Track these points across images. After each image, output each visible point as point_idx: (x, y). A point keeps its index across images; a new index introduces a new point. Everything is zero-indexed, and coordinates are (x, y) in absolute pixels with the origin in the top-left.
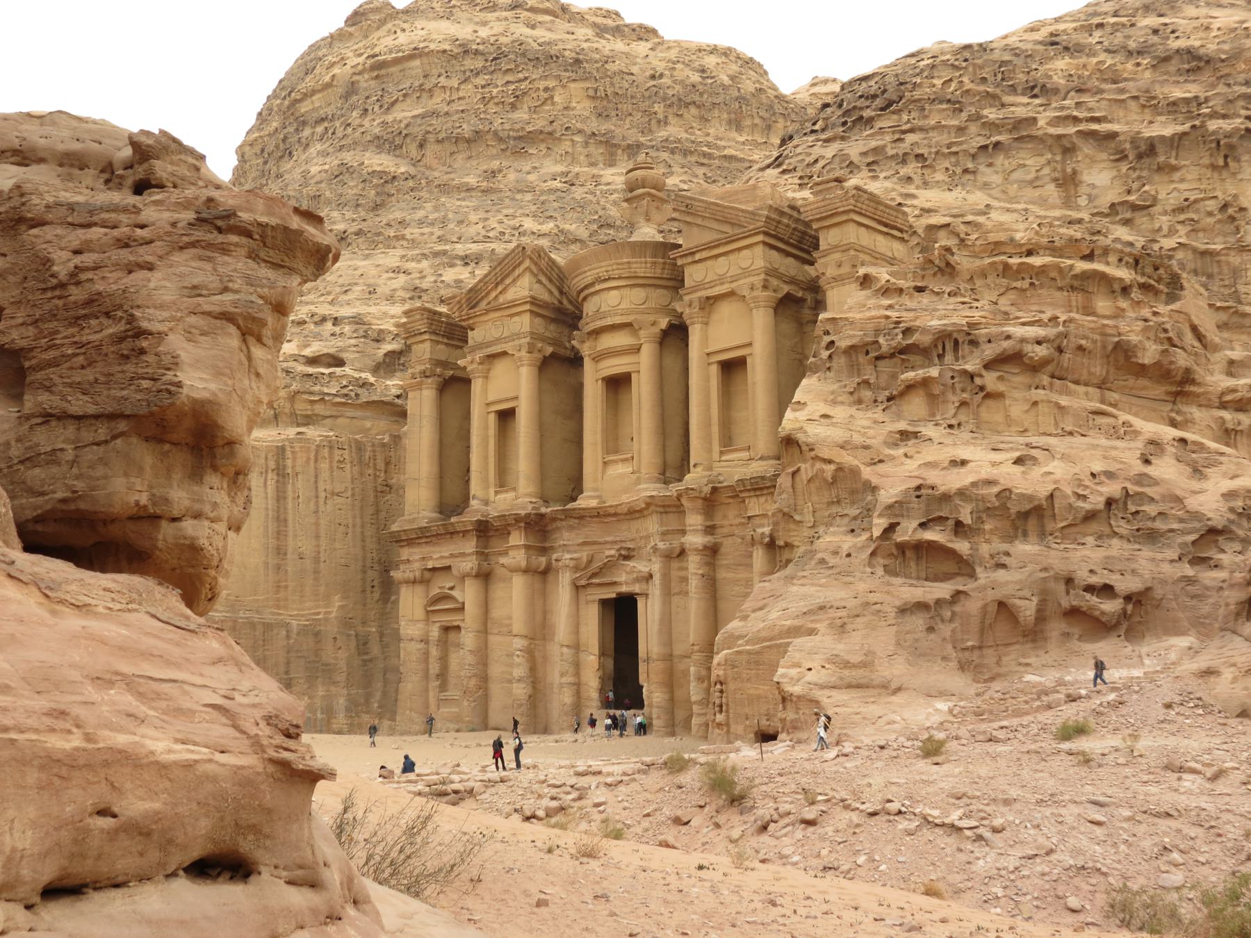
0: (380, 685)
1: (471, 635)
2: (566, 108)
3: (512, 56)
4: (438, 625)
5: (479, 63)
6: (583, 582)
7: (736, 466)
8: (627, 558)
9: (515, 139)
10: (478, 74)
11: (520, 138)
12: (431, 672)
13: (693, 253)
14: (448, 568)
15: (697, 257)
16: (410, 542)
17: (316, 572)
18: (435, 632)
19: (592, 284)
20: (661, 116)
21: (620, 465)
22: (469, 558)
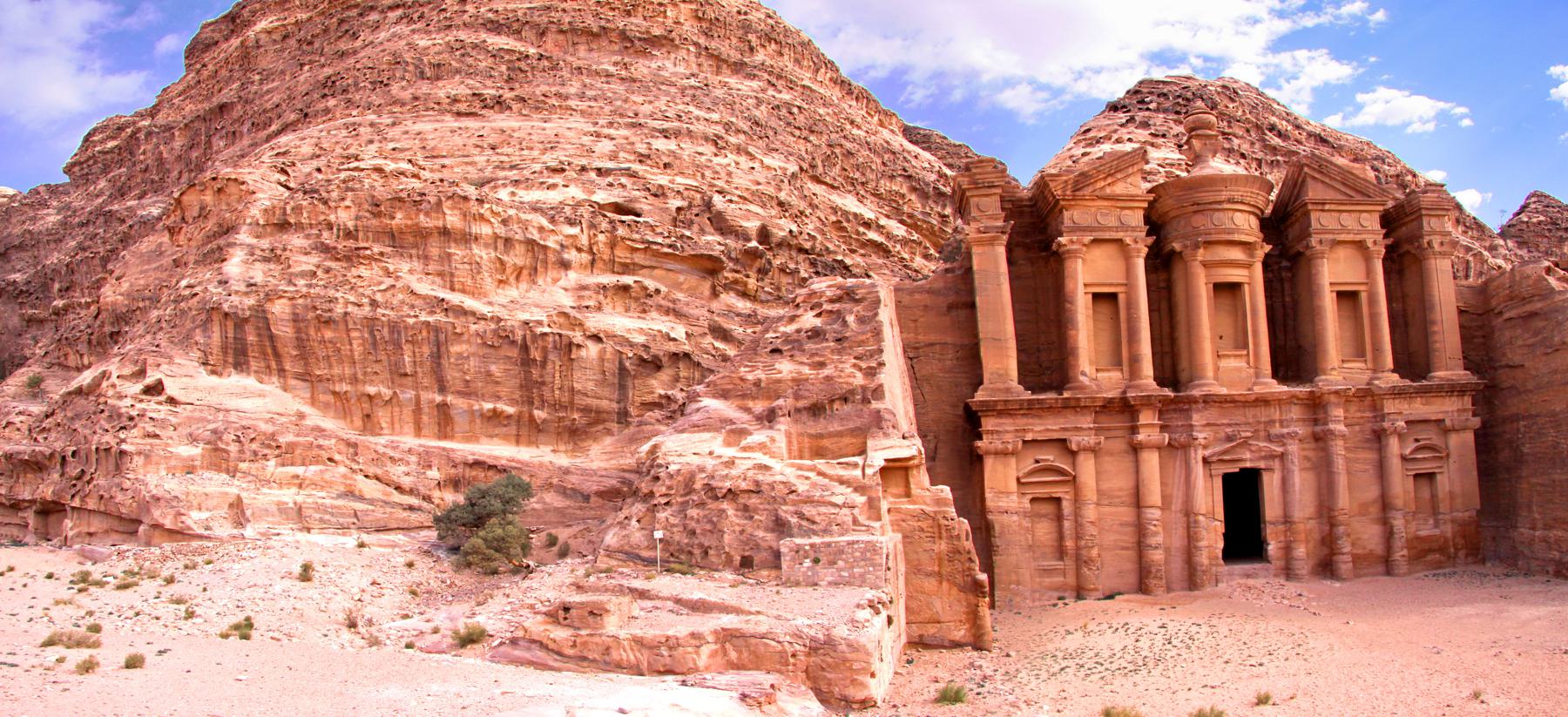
4: (1030, 497)
6: (1215, 459)
16: (1001, 413)
21: (1232, 360)
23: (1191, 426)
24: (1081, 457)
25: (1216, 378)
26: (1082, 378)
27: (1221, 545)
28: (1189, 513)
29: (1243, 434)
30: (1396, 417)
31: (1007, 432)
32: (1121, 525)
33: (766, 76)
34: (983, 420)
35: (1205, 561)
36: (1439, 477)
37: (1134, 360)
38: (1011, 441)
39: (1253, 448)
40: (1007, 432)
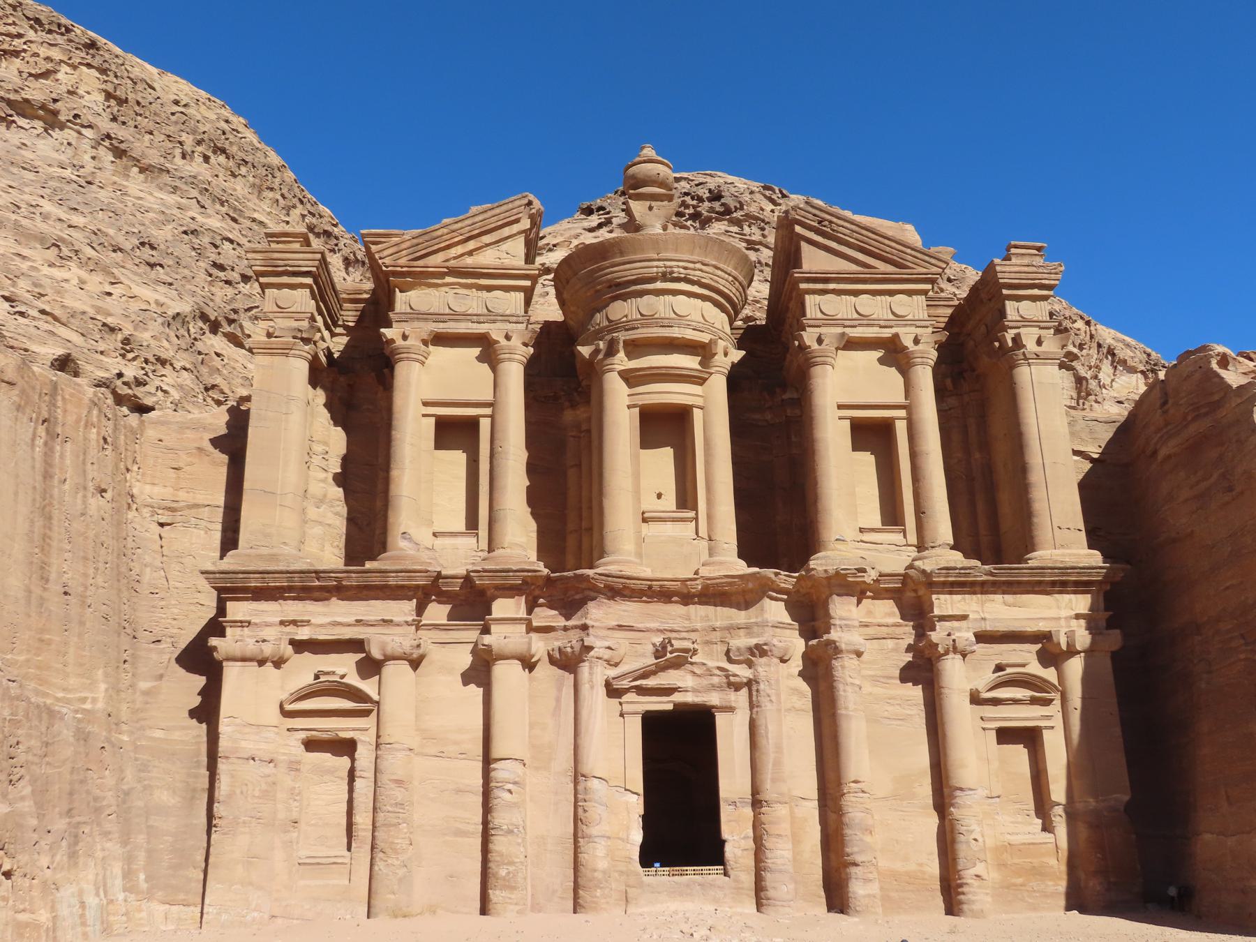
0: (141, 839)
1: (400, 755)
2: (69, 92)
4: (303, 735)
6: (625, 684)
7: (889, 551)
8: (695, 652)
12: (281, 815)
13: (826, 281)
14: (356, 645)
15: (832, 286)
16: (261, 594)
20: (188, 148)
23: (585, 628)
24: (390, 670)
25: (639, 555)
26: (403, 544)
27: (637, 836)
28: (578, 776)
29: (677, 644)
30: (955, 624)
31: (268, 625)
33: (195, 193)
34: (231, 606)
35: (602, 864)
36: (1047, 736)
38: (275, 640)
40: (268, 625)
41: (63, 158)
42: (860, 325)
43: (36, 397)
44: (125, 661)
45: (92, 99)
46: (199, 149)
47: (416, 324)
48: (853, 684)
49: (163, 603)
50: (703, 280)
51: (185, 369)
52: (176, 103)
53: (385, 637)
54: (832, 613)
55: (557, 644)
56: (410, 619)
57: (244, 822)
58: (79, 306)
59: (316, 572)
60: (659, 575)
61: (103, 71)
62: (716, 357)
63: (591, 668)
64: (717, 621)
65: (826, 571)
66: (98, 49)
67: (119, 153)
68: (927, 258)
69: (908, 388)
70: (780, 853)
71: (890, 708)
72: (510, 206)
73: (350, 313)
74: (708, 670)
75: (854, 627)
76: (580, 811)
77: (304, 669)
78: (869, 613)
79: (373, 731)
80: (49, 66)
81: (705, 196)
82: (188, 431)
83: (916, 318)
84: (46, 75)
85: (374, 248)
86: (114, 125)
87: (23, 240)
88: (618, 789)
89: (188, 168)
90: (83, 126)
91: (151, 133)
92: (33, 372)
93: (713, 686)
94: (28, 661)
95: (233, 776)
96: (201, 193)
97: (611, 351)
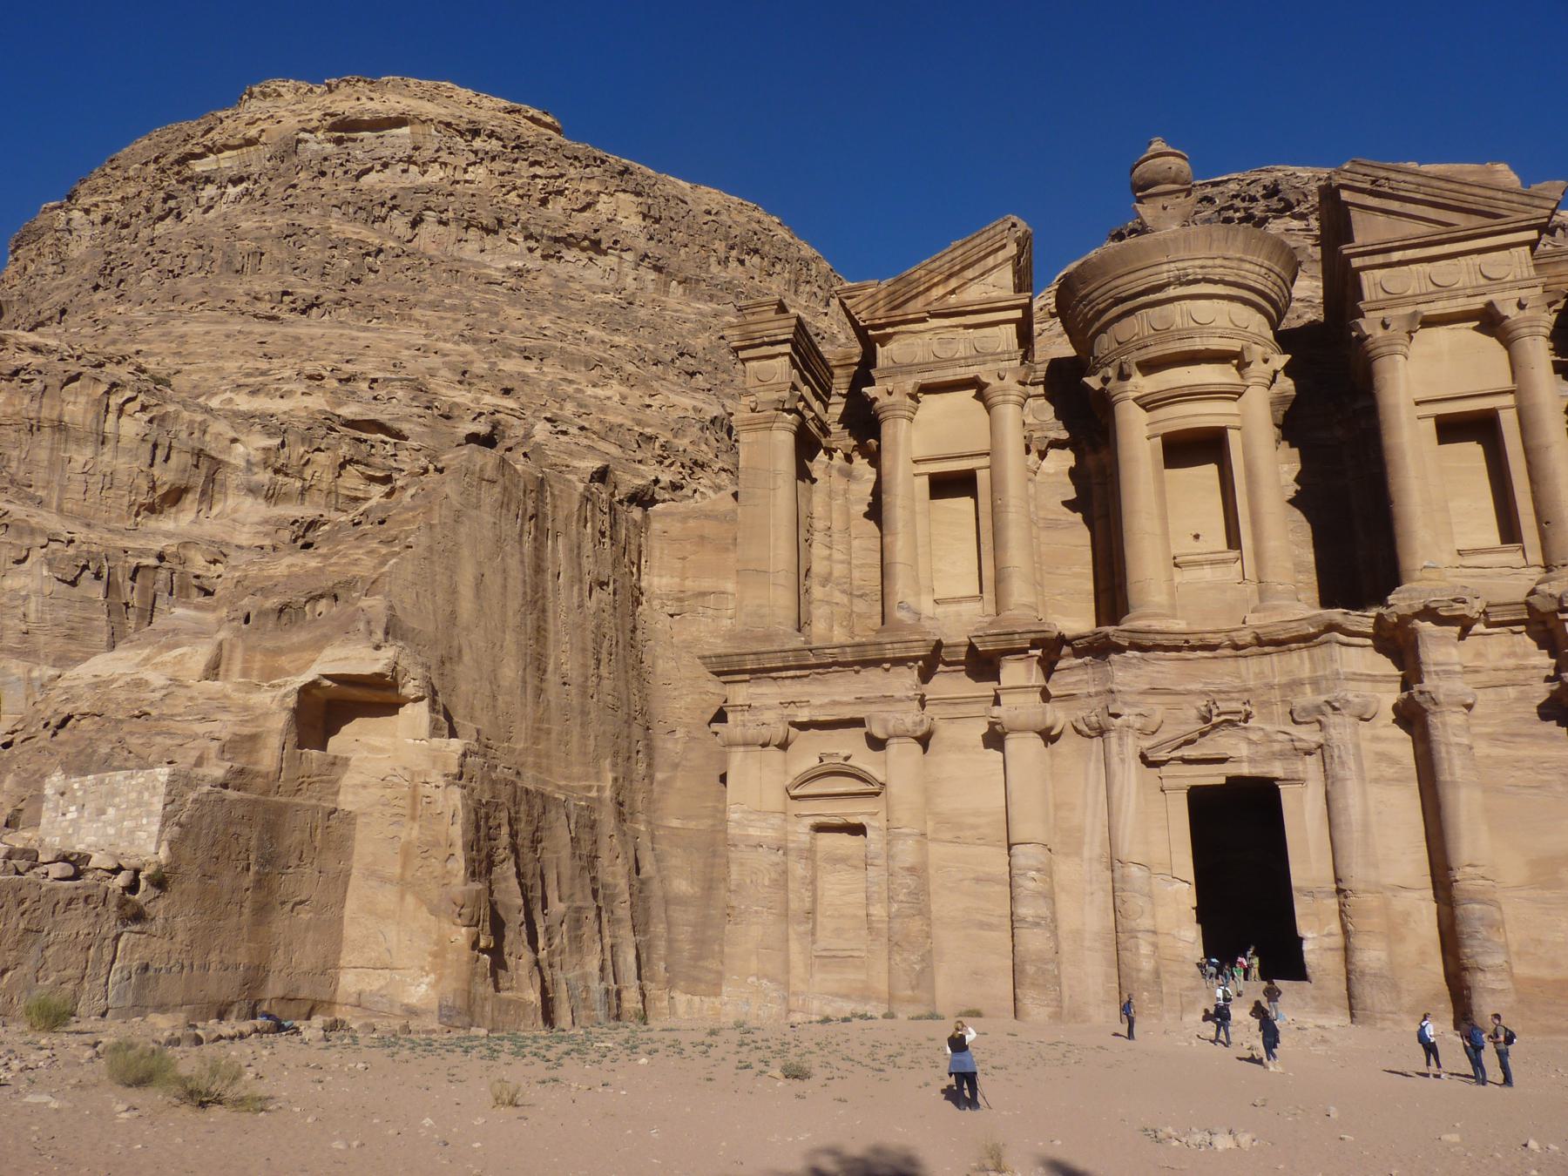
2: (610, 220)
3: (543, 148)
5: (495, 145)
6: (1162, 755)
7: (1500, 575)
8: (1248, 716)
9: (550, 238)
10: (493, 159)
11: (557, 240)
12: (794, 905)
15: (1396, 256)
17: (584, 713)
18: (801, 832)
19: (1160, 288)
22: (900, 706)
24: (894, 747)
28: (1114, 862)
29: (1224, 706)
32: (978, 880)
35: (1147, 965)
37: (999, 580)
39: (1254, 736)
41: (607, 283)
42: (1439, 299)
43: (521, 494)
44: (638, 752)
45: (631, 222)
46: (734, 253)
47: (899, 378)
48: (1459, 745)
49: (676, 693)
50: (1227, 278)
51: (724, 470)
52: (709, 213)
53: (885, 715)
54: (1423, 657)
55: (1081, 714)
56: (911, 694)
57: (756, 912)
58: (619, 420)
59: (810, 650)
60: (1196, 628)
61: (638, 194)
62: (1252, 366)
63: (1120, 738)
64: (1274, 677)
65: (1410, 606)
66: (631, 174)
67: (658, 269)
68: (1526, 200)
69: (1515, 367)
70: (1371, 955)
71: (1520, 773)
72: (992, 232)
73: (842, 380)
74: (1267, 735)
75: (1455, 673)
76: (1118, 902)
77: (809, 752)
78: (1479, 655)
79: (882, 815)
80: (589, 199)
81: (1258, 195)
82: (691, 521)
83: (1519, 277)
84: (588, 206)
85: (848, 302)
86: (652, 243)
87: (569, 366)
88: (1165, 877)
89: (723, 274)
90: (622, 250)
91: (686, 246)
92: (515, 470)
93: (1274, 754)
94: (527, 749)
95: (742, 864)
96: (737, 297)
97: (1123, 376)
